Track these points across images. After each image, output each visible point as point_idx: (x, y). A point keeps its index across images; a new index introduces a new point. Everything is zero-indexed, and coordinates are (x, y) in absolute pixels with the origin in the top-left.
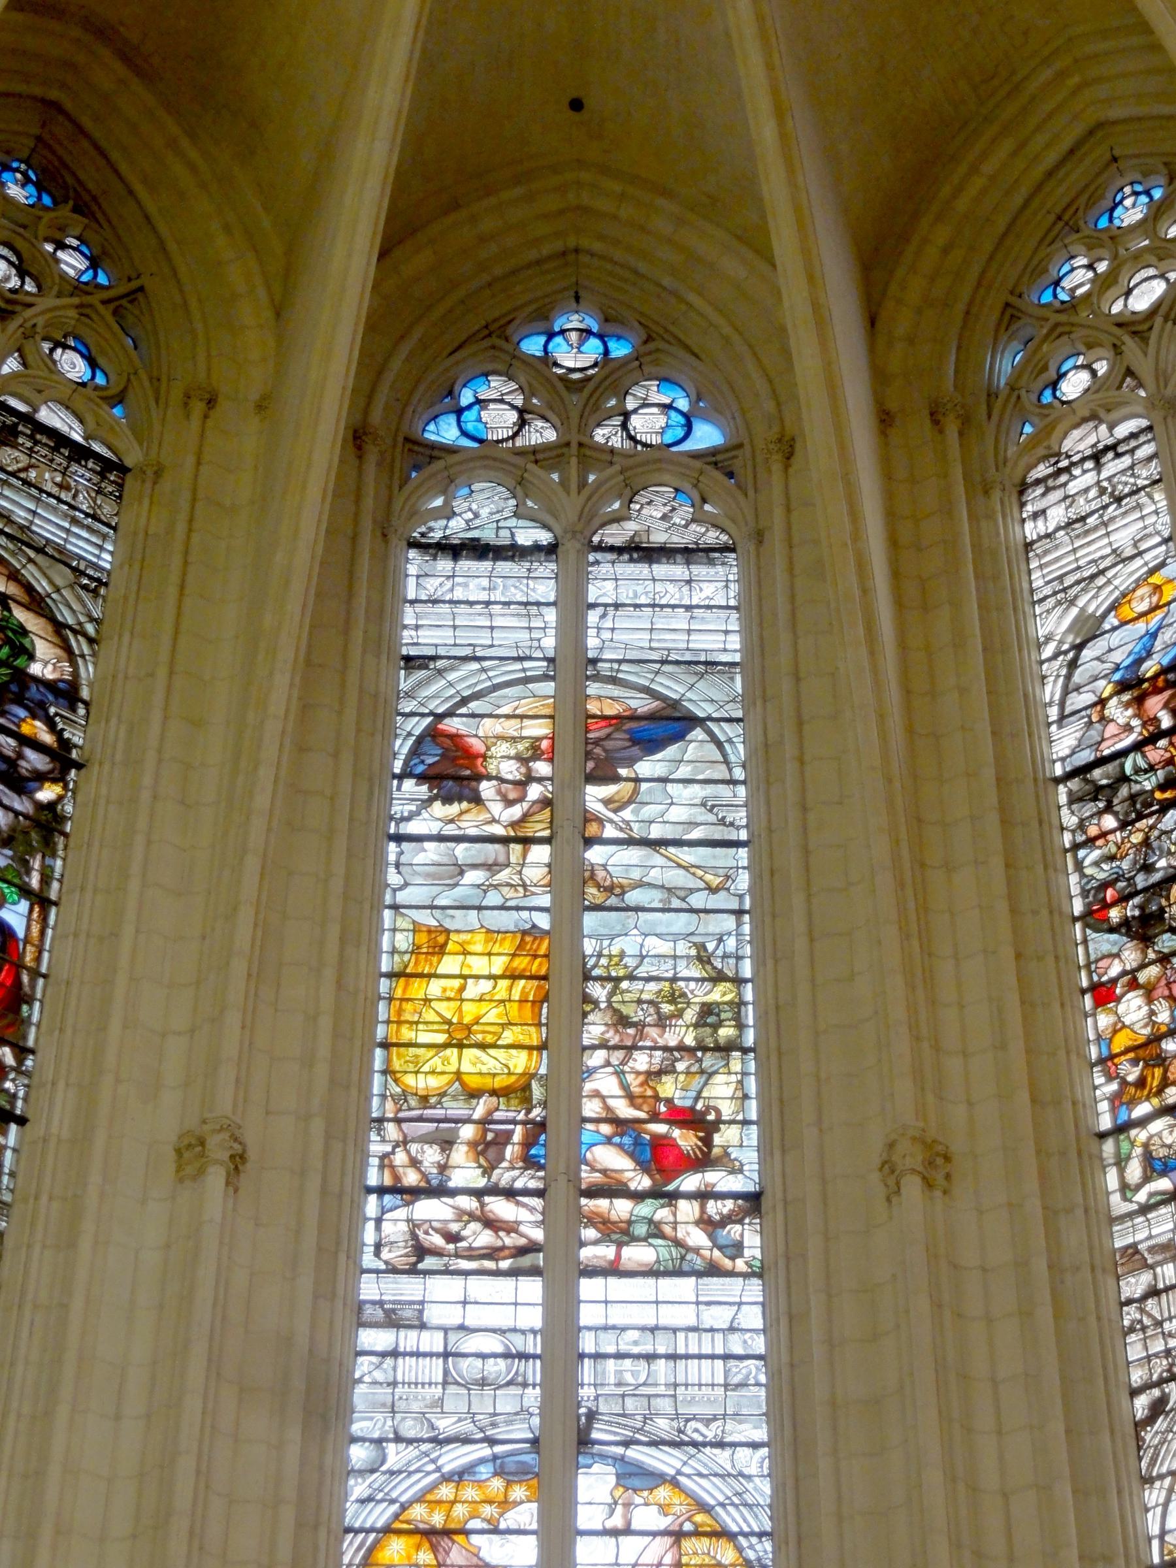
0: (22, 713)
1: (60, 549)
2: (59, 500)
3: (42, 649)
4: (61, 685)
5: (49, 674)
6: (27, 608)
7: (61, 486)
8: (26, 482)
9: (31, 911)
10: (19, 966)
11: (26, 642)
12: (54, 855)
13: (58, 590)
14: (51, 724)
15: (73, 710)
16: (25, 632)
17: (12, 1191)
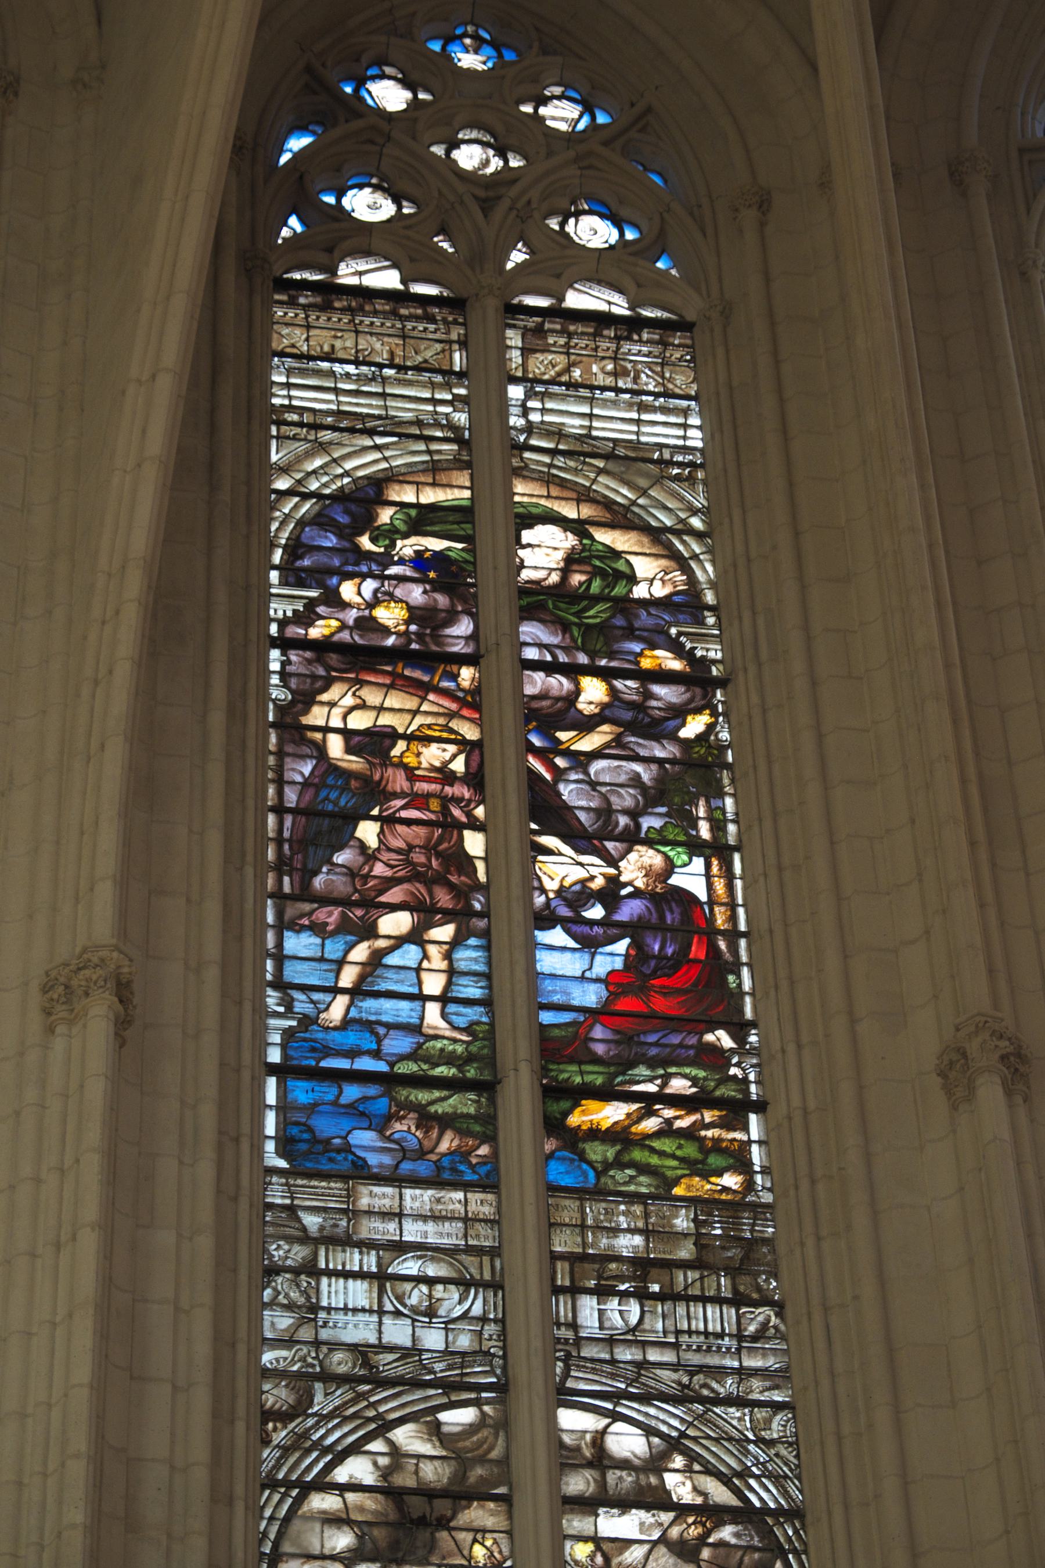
0: (637, 647)
1: (636, 445)
2: (618, 390)
3: (644, 567)
4: (676, 599)
5: (660, 591)
6: (612, 526)
7: (615, 374)
8: (571, 385)
9: (708, 866)
10: (711, 932)
11: (621, 566)
12: (721, 795)
13: (644, 493)
14: (676, 648)
15: (701, 623)
16: (616, 554)
17: (769, 1190)
